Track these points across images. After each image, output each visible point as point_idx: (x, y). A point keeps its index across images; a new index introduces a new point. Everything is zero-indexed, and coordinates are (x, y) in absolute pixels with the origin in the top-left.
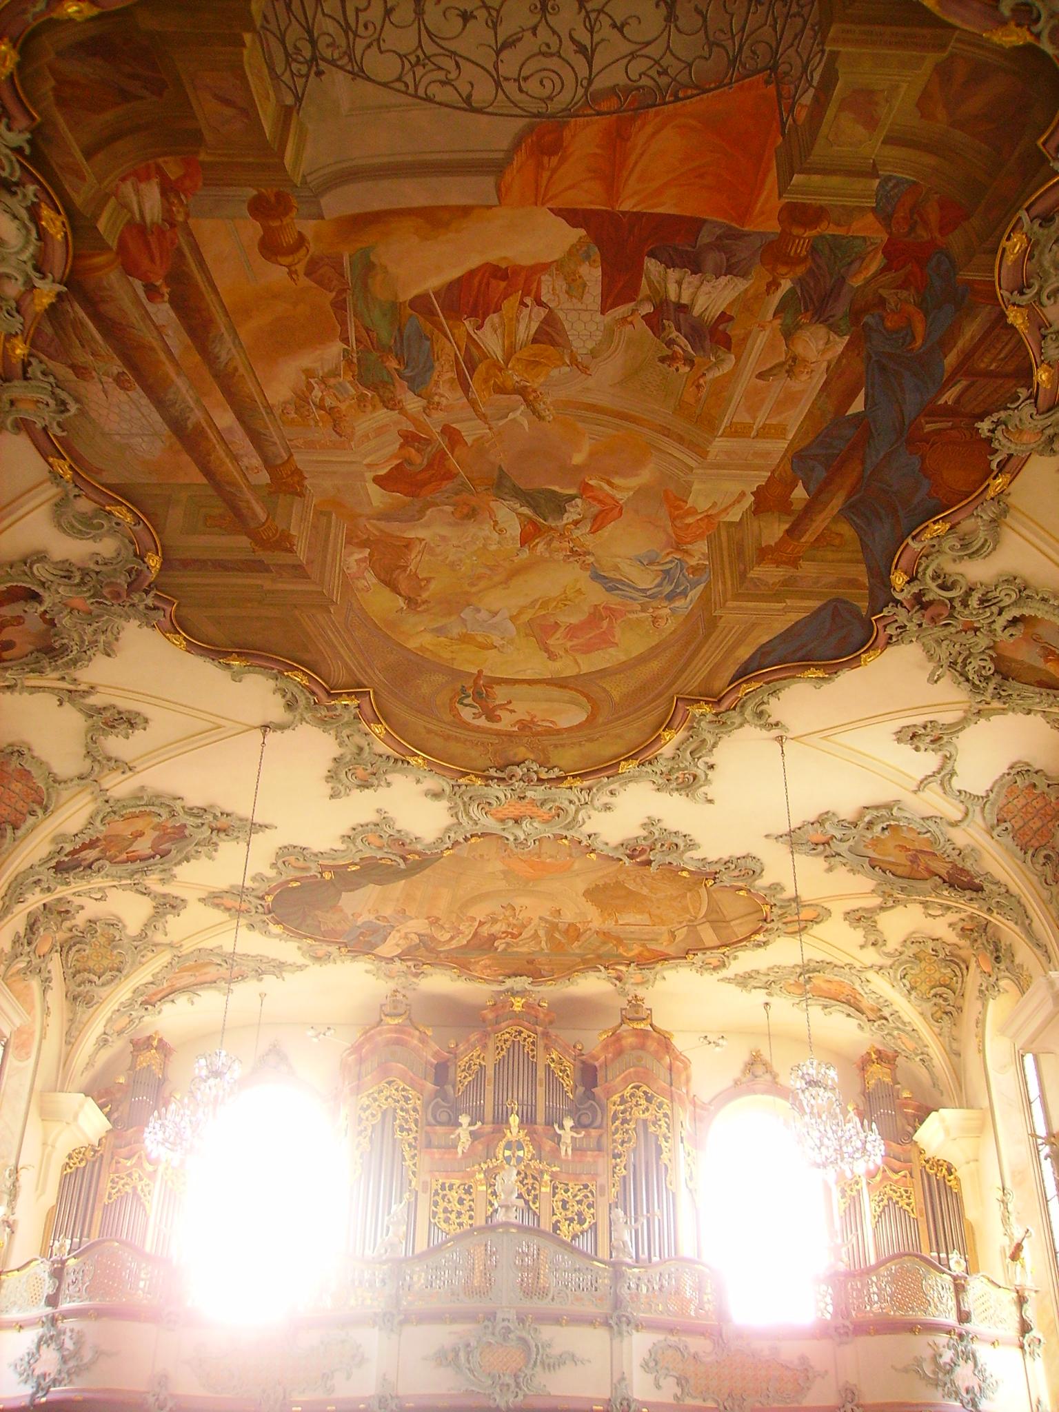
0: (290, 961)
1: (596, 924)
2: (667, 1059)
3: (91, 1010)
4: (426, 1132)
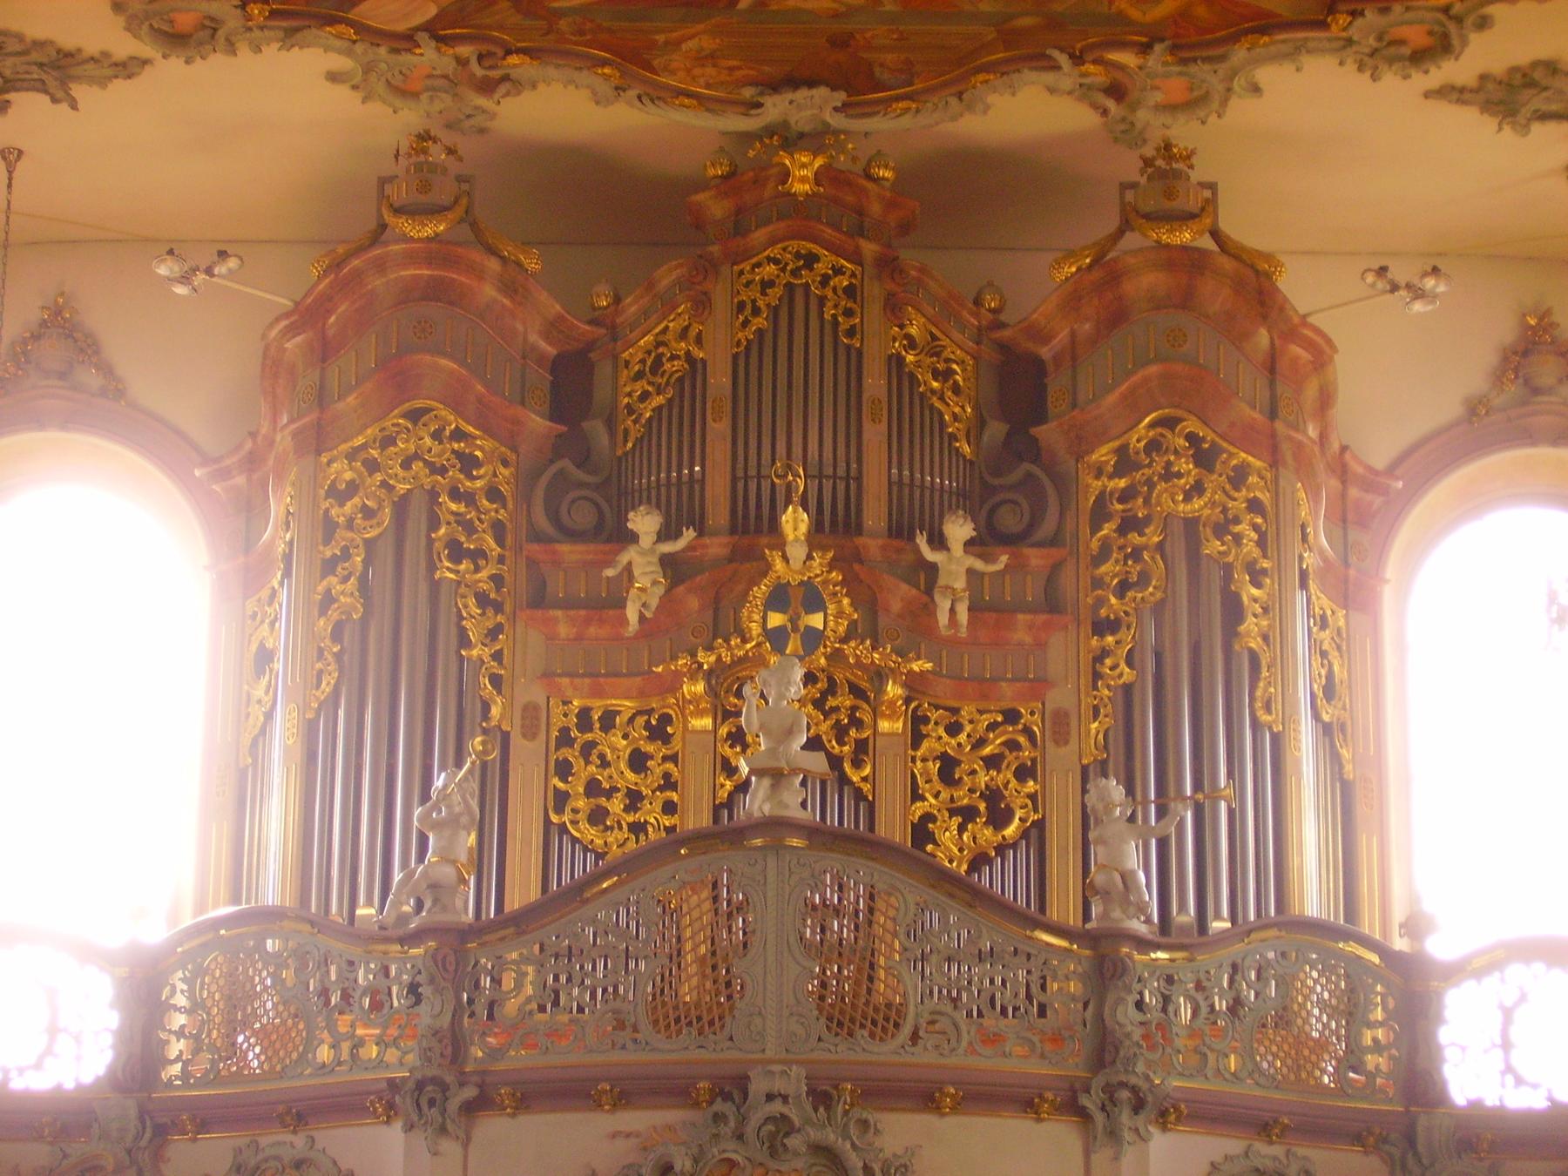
0: (92, 47)
2: (1263, 338)
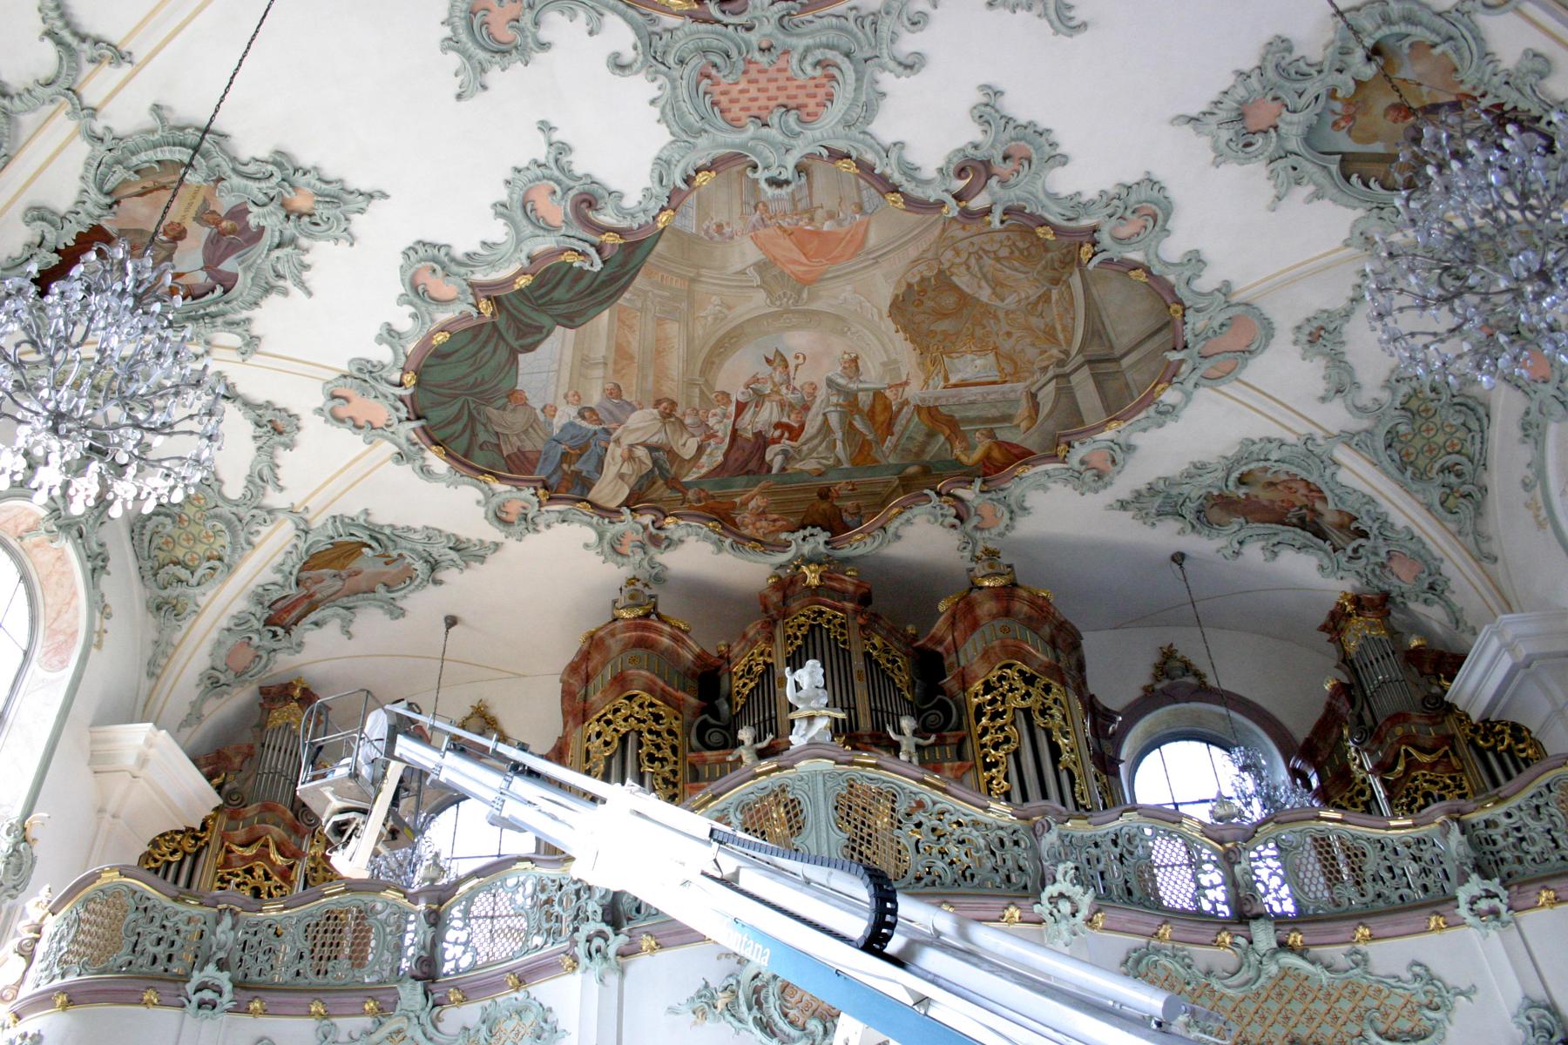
1: (914, 392)
3: (185, 625)
4: (692, 765)
